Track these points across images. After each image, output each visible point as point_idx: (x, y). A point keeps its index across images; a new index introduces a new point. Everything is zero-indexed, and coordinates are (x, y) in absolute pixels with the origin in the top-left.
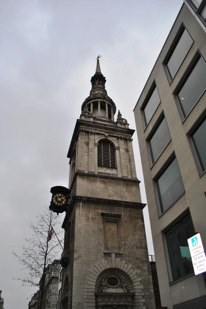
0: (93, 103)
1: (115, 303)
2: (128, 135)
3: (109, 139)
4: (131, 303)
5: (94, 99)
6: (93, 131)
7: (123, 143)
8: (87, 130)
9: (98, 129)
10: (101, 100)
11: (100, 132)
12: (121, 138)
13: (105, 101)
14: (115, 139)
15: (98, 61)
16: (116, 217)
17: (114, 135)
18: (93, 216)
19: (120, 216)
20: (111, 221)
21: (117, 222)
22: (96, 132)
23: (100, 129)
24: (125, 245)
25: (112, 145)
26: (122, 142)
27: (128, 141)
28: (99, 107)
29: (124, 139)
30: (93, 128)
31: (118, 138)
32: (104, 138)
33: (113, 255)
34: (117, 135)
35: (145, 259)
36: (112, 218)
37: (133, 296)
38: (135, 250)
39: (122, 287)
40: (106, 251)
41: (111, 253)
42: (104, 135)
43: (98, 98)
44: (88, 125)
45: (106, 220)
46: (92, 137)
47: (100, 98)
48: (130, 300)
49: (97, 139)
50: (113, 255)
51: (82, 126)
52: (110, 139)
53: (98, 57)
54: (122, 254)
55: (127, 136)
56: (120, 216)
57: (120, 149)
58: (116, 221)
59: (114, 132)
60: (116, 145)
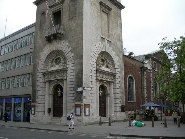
1: (105, 79)
4: (113, 81)
16: (108, 9)
18: (95, 2)
19: (110, 9)
20: (105, 11)
21: (107, 14)
24: (112, 35)
33: (106, 41)
35: (121, 50)
36: (106, 10)
37: (114, 75)
38: (117, 41)
39: (107, 67)
40: (102, 36)
41: (105, 39)
45: (103, 10)
48: (113, 78)
50: (106, 41)
54: (110, 42)
56: (110, 9)
58: (108, 13)
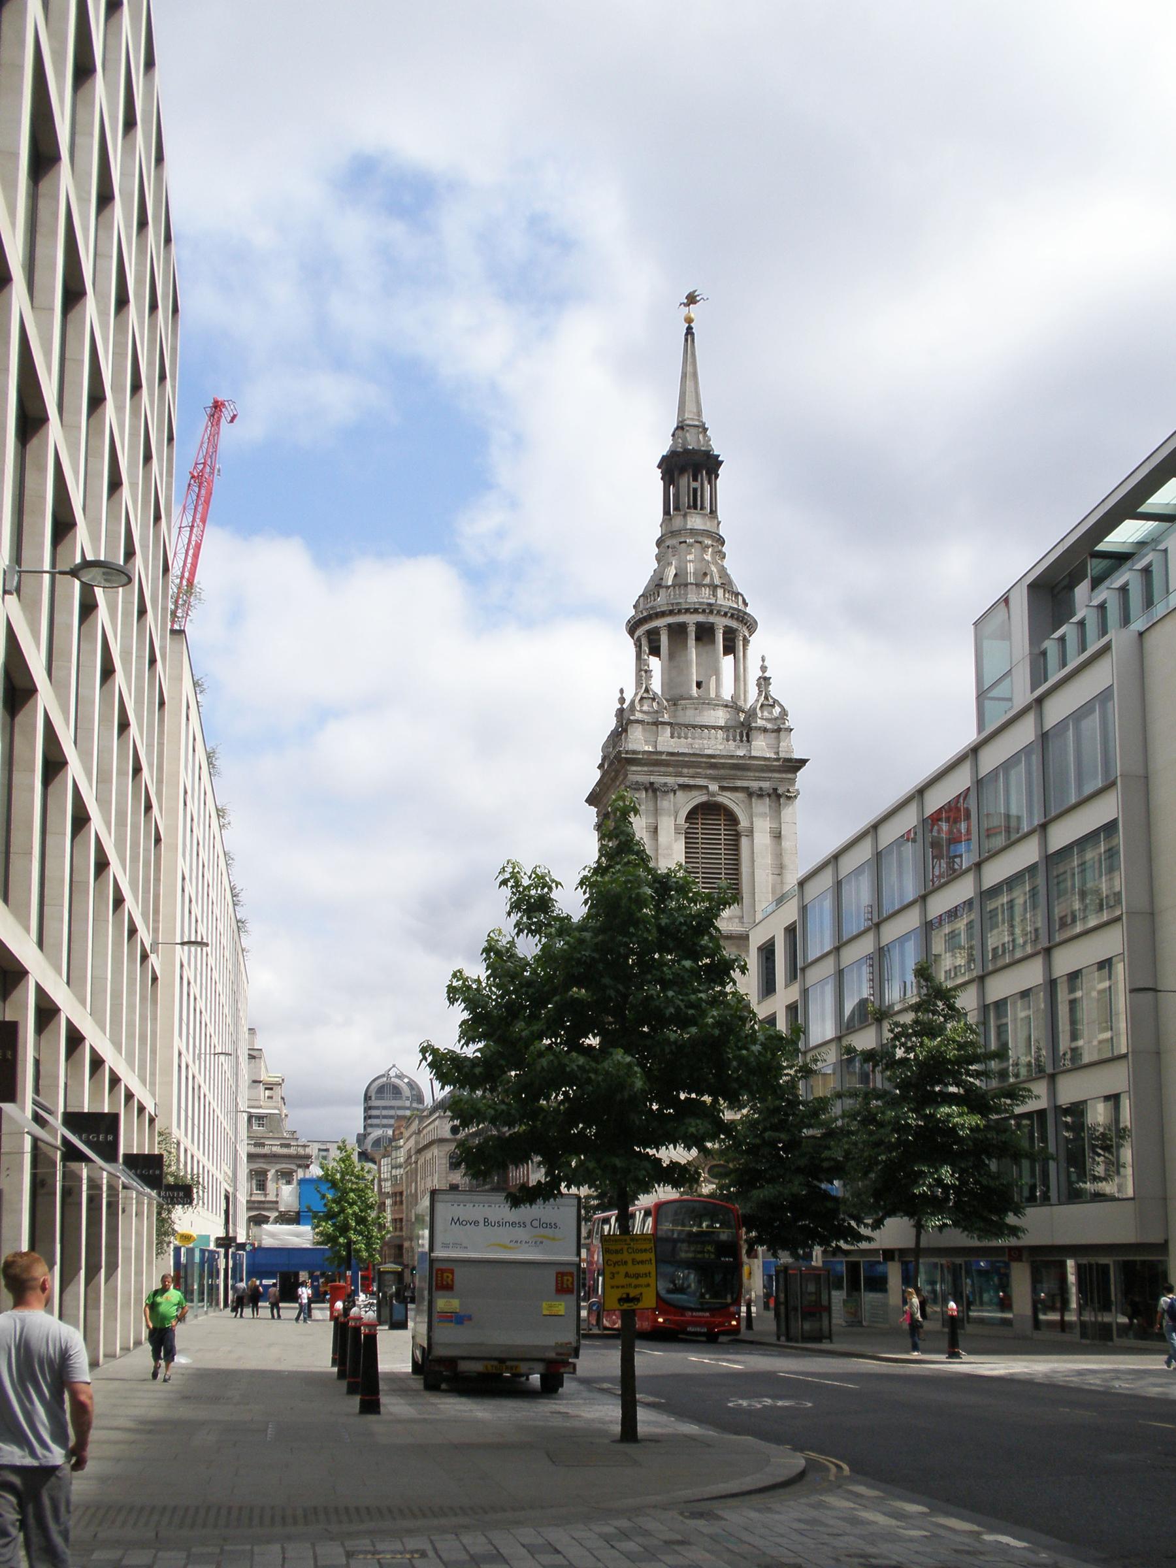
0: (669, 626)
2: (784, 776)
3: (720, 799)
5: (671, 613)
6: (670, 780)
7: (767, 810)
8: (653, 779)
9: (685, 771)
10: (701, 618)
11: (692, 782)
12: (761, 794)
13: (711, 619)
14: (741, 796)
15: (689, 331)
17: (739, 783)
22: (681, 780)
23: (692, 771)
25: (732, 819)
26: (762, 806)
27: (782, 800)
28: (692, 642)
29: (769, 795)
30: (671, 769)
31: (750, 793)
32: (704, 798)
34: (745, 784)
42: (707, 787)
43: (687, 611)
44: (655, 761)
46: (666, 803)
47: (696, 611)
49: (686, 802)
51: (634, 768)
52: (725, 799)
53: (692, 299)
55: (782, 780)
57: (756, 835)
59: (739, 773)
60: (744, 823)
